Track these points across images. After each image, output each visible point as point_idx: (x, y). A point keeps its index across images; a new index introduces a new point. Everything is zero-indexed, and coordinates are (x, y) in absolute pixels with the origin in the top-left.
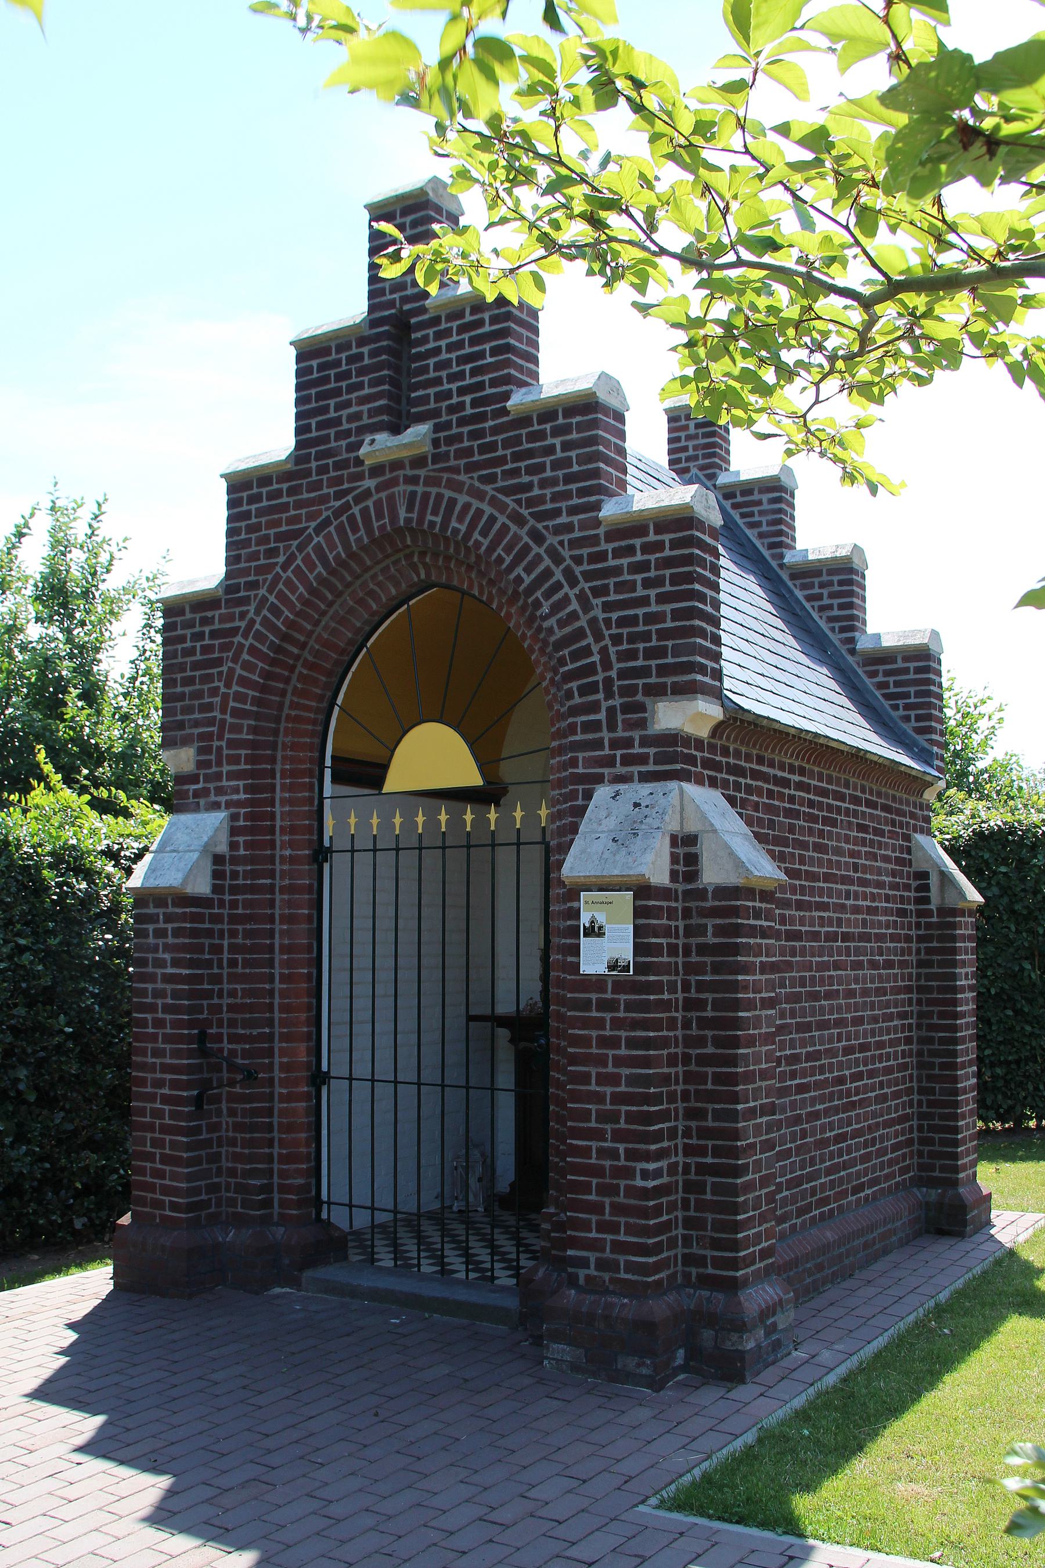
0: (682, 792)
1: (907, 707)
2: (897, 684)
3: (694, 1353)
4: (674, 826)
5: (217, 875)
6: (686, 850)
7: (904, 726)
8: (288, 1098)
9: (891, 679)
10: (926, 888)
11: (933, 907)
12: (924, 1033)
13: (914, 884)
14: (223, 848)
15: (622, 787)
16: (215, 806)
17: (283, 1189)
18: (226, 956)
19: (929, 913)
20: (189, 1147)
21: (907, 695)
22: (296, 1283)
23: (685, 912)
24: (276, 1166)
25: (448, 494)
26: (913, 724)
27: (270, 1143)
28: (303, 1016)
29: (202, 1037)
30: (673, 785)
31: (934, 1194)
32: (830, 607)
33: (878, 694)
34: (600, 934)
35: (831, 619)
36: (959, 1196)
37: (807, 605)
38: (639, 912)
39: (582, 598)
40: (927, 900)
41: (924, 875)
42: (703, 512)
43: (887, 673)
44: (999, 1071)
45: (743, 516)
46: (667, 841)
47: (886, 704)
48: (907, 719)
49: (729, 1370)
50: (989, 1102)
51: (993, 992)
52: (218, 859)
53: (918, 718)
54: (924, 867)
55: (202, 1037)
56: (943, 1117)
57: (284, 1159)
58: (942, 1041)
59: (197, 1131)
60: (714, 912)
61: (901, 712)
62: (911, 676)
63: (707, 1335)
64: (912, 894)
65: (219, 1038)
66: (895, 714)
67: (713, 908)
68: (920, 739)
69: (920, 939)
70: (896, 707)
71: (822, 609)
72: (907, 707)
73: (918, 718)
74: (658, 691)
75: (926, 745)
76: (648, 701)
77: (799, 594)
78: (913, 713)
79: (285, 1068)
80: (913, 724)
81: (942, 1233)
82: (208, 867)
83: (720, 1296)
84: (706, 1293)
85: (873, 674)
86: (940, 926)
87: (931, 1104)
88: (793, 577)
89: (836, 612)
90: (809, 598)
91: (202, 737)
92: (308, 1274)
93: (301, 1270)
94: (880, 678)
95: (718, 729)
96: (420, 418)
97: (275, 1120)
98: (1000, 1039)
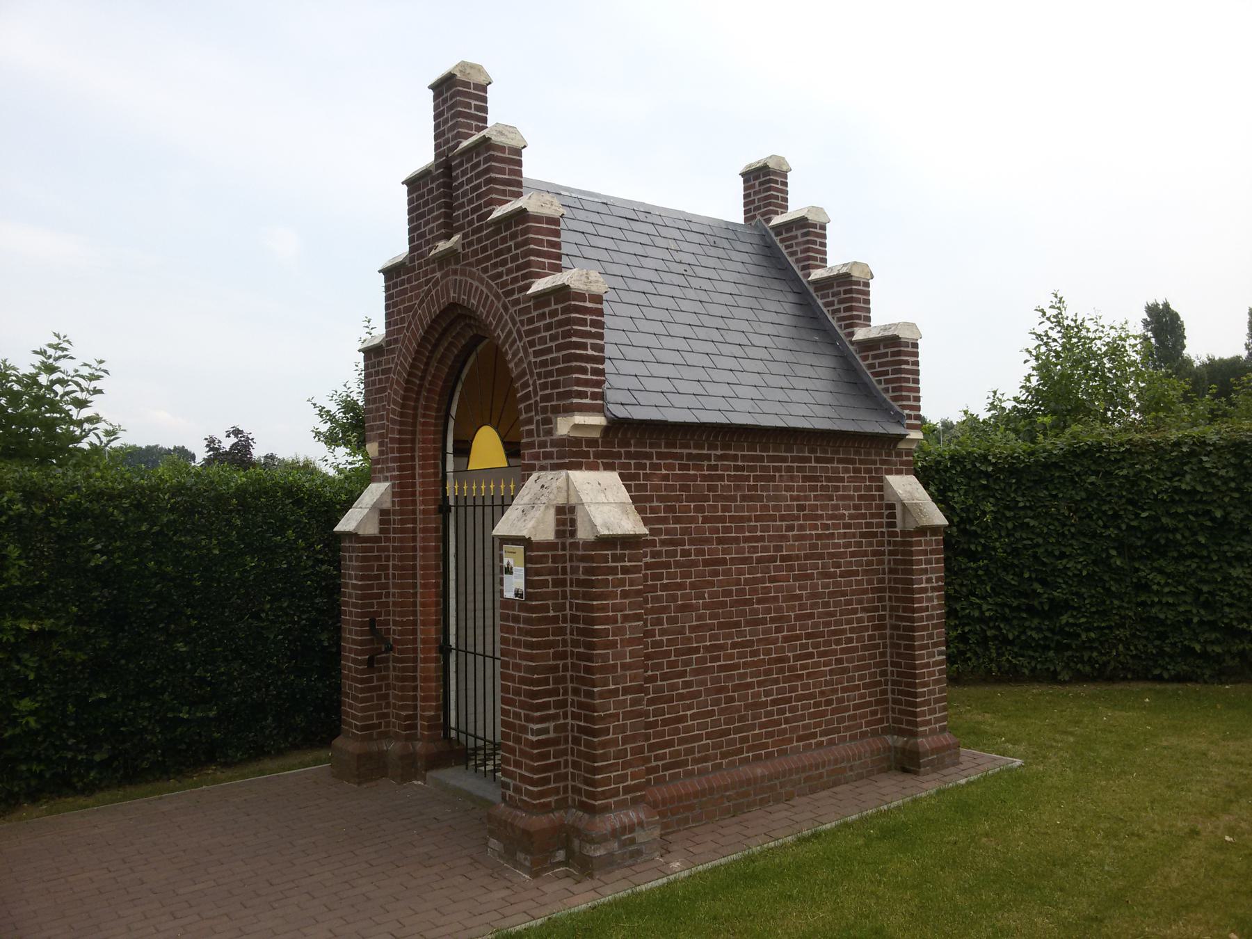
0: (568, 477)
1: (887, 381)
2: (881, 365)
3: (570, 854)
4: (561, 500)
5: (381, 522)
6: (566, 515)
7: (885, 396)
8: (425, 660)
9: (877, 362)
10: (893, 516)
11: (898, 530)
12: (894, 622)
13: (886, 512)
14: (387, 505)
15: (543, 473)
16: (386, 479)
17: (423, 718)
18: (391, 571)
19: (895, 534)
20: (362, 691)
21: (886, 373)
22: (424, 779)
23: (569, 558)
24: (419, 703)
25: (470, 280)
26: (891, 394)
27: (415, 689)
28: (433, 609)
29: (372, 623)
30: (563, 473)
31: (900, 741)
32: (838, 310)
33: (868, 372)
34: (511, 573)
35: (840, 319)
36: (916, 743)
37: (825, 310)
38: (527, 560)
39: (524, 348)
40: (893, 525)
41: (892, 506)
42: (582, 287)
43: (875, 357)
44: (1093, 635)
45: (787, 247)
46: (552, 512)
47: (874, 379)
48: (886, 390)
49: (585, 868)
50: (1086, 658)
51: (1084, 573)
52: (383, 512)
53: (894, 390)
54: (892, 500)
55: (372, 623)
56: (908, 685)
57: (424, 699)
58: (906, 629)
59: (370, 680)
60: (583, 559)
61: (883, 386)
62: (889, 359)
63: (576, 843)
64: (885, 520)
65: (387, 623)
66: (879, 387)
67: (583, 556)
68: (895, 405)
69: (891, 553)
70: (879, 382)
71: (834, 312)
72: (887, 381)
73: (894, 390)
74: (557, 411)
75: (899, 409)
76: (552, 416)
77: (820, 302)
78: (890, 386)
79: (424, 642)
80: (891, 394)
81: (905, 770)
82: (376, 518)
83: (586, 816)
84: (580, 813)
85: (865, 358)
86: (904, 543)
87: (899, 674)
88: (816, 290)
89: (843, 314)
90: (826, 305)
91: (381, 436)
92: (429, 774)
93: (426, 770)
94: (870, 361)
95: (606, 430)
96: (457, 232)
97: (418, 674)
98: (1093, 609)
